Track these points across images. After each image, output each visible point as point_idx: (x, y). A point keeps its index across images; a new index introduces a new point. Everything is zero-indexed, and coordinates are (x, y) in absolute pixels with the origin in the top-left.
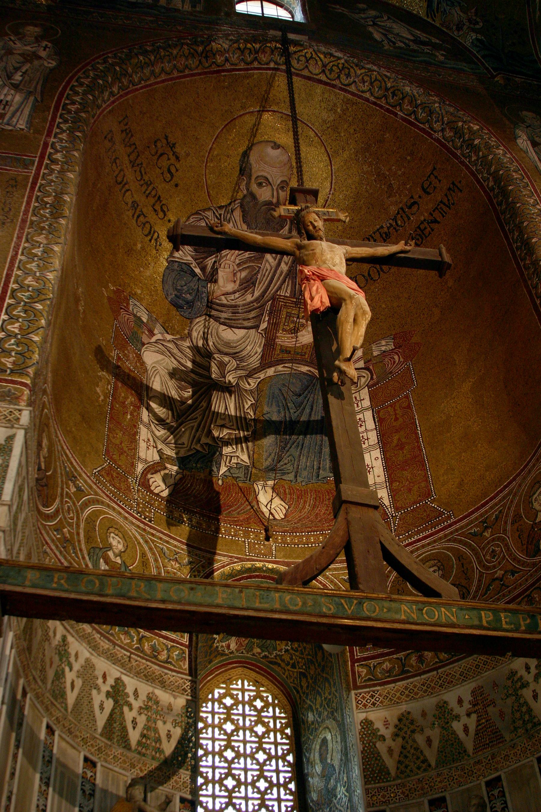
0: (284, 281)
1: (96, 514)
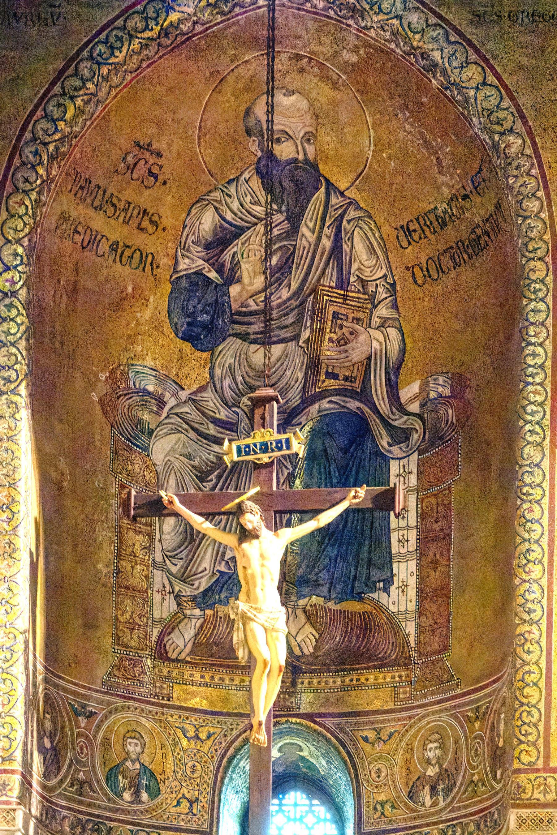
0: (327, 264)
1: (110, 729)
